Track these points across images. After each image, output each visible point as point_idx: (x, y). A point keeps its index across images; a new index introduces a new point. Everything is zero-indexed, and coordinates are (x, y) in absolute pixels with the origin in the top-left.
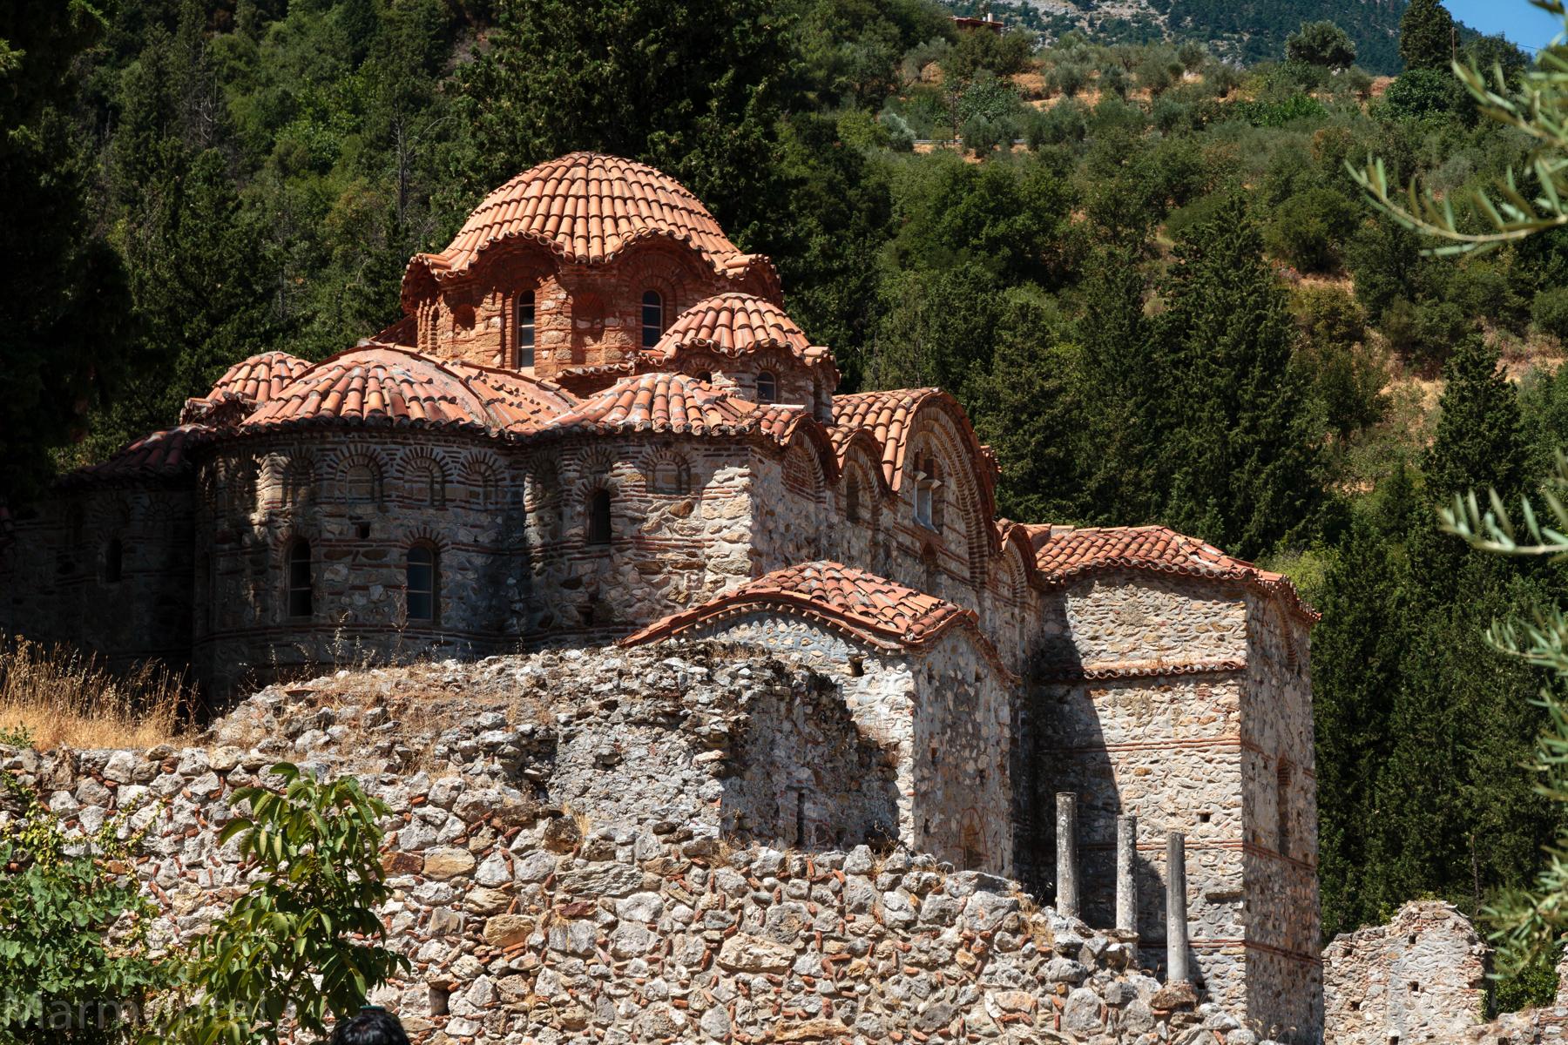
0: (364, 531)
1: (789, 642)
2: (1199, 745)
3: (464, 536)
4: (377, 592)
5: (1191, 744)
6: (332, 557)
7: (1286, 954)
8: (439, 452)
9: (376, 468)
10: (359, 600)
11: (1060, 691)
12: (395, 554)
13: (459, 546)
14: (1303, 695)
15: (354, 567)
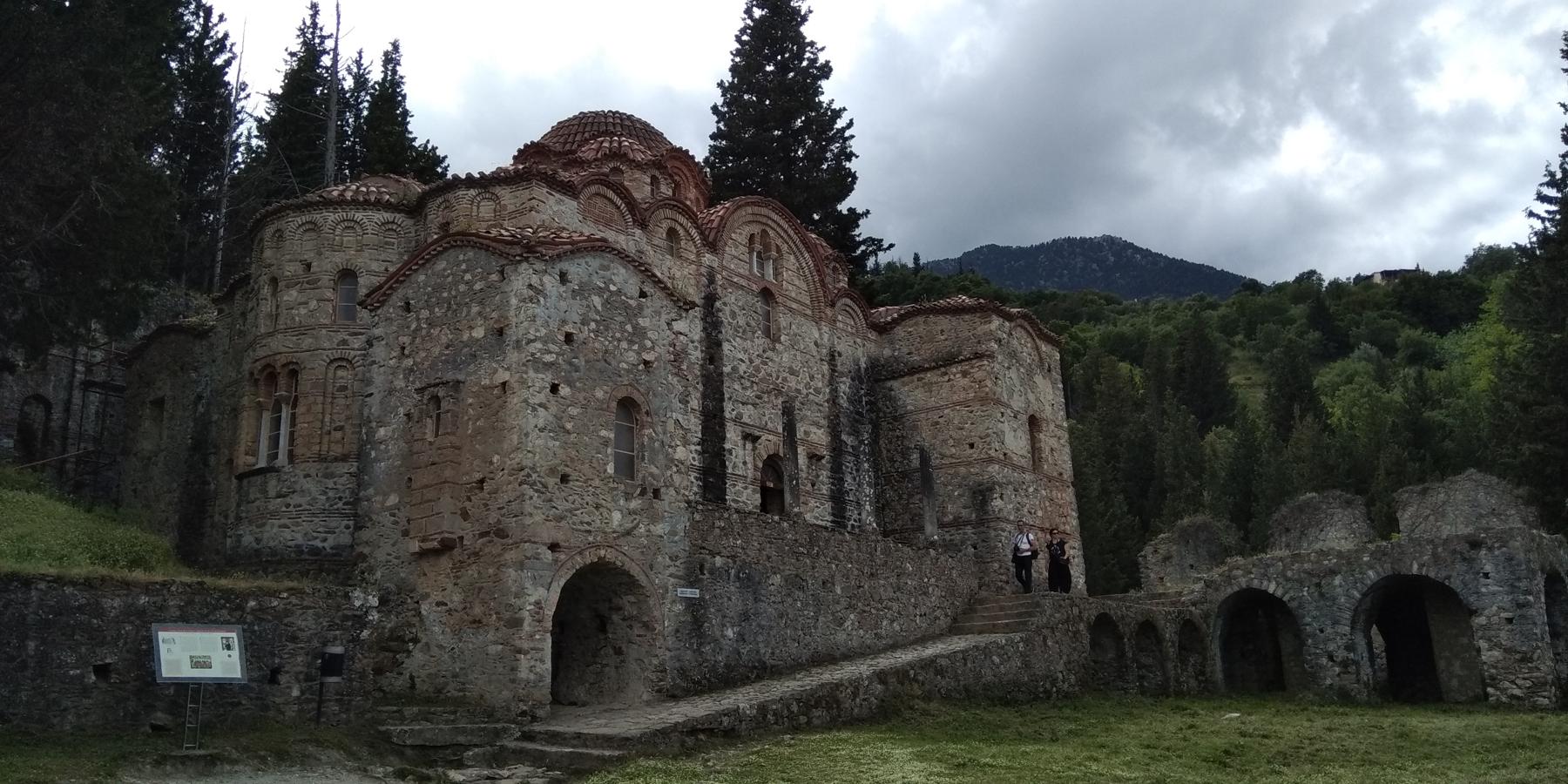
0: (309, 266)
1: (464, 267)
2: (965, 403)
3: (375, 266)
4: (313, 304)
5: (959, 403)
6: (288, 287)
7: (1042, 530)
8: (359, 216)
9: (314, 227)
10: (303, 311)
11: (889, 384)
12: (325, 280)
13: (370, 272)
14: (1054, 383)
15: (300, 291)
